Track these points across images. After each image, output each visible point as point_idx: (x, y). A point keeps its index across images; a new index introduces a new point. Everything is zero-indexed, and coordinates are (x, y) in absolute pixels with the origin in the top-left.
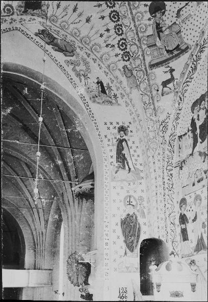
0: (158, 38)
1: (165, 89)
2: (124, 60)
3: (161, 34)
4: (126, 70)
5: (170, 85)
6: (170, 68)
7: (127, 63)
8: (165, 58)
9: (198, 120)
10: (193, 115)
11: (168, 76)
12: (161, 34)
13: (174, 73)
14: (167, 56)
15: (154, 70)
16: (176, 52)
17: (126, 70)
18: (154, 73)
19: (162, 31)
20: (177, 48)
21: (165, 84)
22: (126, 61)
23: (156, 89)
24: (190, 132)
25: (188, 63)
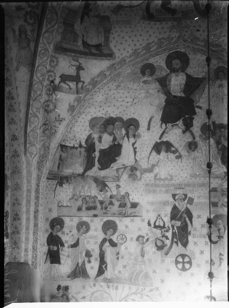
0: (80, 19)
1: (63, 84)
2: (26, 21)
3: (86, 17)
4: (23, 36)
5: (72, 85)
6: (78, 64)
7: (29, 28)
8: (76, 49)
9: (100, 141)
10: (91, 132)
11: (72, 71)
12: (86, 17)
13: (81, 72)
14: (81, 48)
15: (56, 55)
16: (94, 51)
17: (23, 36)
18: (57, 58)
19: (88, 15)
20: (98, 47)
21: (65, 78)
22: (29, 24)
23: (51, 79)
24: (83, 150)
25: (107, 73)
